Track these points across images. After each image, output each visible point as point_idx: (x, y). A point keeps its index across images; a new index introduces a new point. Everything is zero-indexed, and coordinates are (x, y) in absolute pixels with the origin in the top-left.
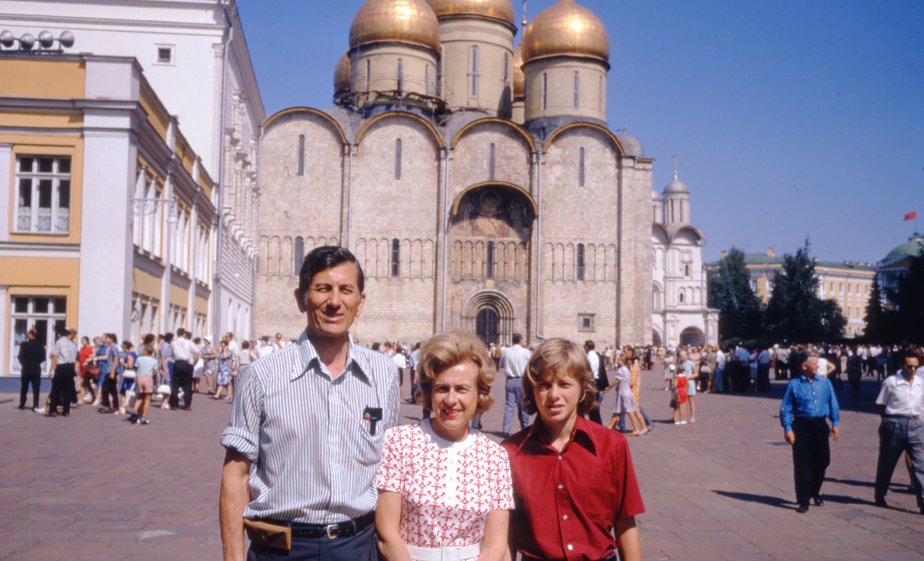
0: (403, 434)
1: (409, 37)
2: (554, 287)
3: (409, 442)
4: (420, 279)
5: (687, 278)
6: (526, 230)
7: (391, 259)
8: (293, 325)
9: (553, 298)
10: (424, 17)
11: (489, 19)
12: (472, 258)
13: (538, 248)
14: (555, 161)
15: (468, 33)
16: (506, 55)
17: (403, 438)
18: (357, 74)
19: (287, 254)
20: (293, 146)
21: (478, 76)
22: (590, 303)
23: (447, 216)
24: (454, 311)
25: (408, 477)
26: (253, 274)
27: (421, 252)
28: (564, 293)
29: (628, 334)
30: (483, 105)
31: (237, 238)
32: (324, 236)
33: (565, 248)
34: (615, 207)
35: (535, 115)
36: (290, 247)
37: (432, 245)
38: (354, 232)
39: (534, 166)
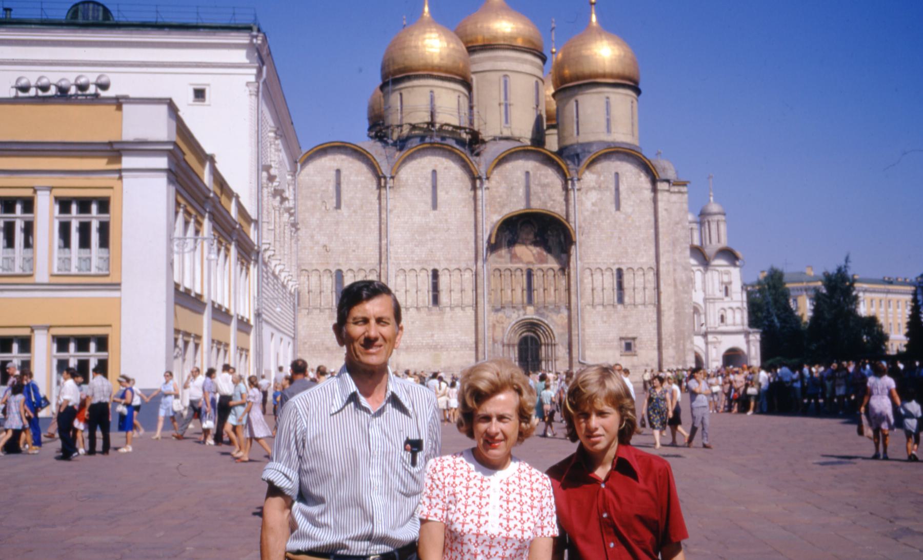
0: (445, 464)
1: (439, 68)
2: (594, 312)
3: (452, 472)
5: (727, 299)
6: (564, 256)
7: (431, 289)
10: (454, 49)
12: (512, 286)
15: (499, 63)
17: (446, 468)
18: (390, 107)
19: (327, 287)
21: (510, 105)
23: (485, 245)
25: (451, 506)
26: (294, 307)
30: (517, 134)
31: (277, 273)
32: (363, 268)
33: (604, 272)
34: (652, 231)
35: (568, 142)
36: (330, 280)
37: (471, 274)
38: (393, 264)
39: (570, 192)
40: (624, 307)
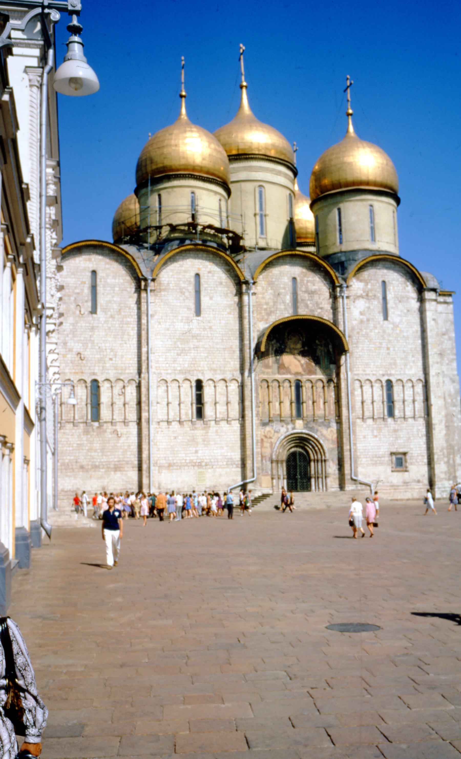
1: (201, 169)
2: (365, 426)
4: (226, 421)
7: (194, 401)
8: (91, 477)
9: (364, 437)
11: (273, 159)
12: (280, 398)
13: (347, 385)
14: (358, 295)
16: (290, 194)
18: (149, 207)
21: (265, 216)
22: (402, 441)
24: (264, 455)
27: (226, 393)
28: (375, 431)
29: (442, 472)
32: (122, 378)
33: (374, 384)
34: (420, 342)
36: (85, 391)
37: (237, 385)
38: (155, 373)
39: (338, 299)
40: (395, 421)
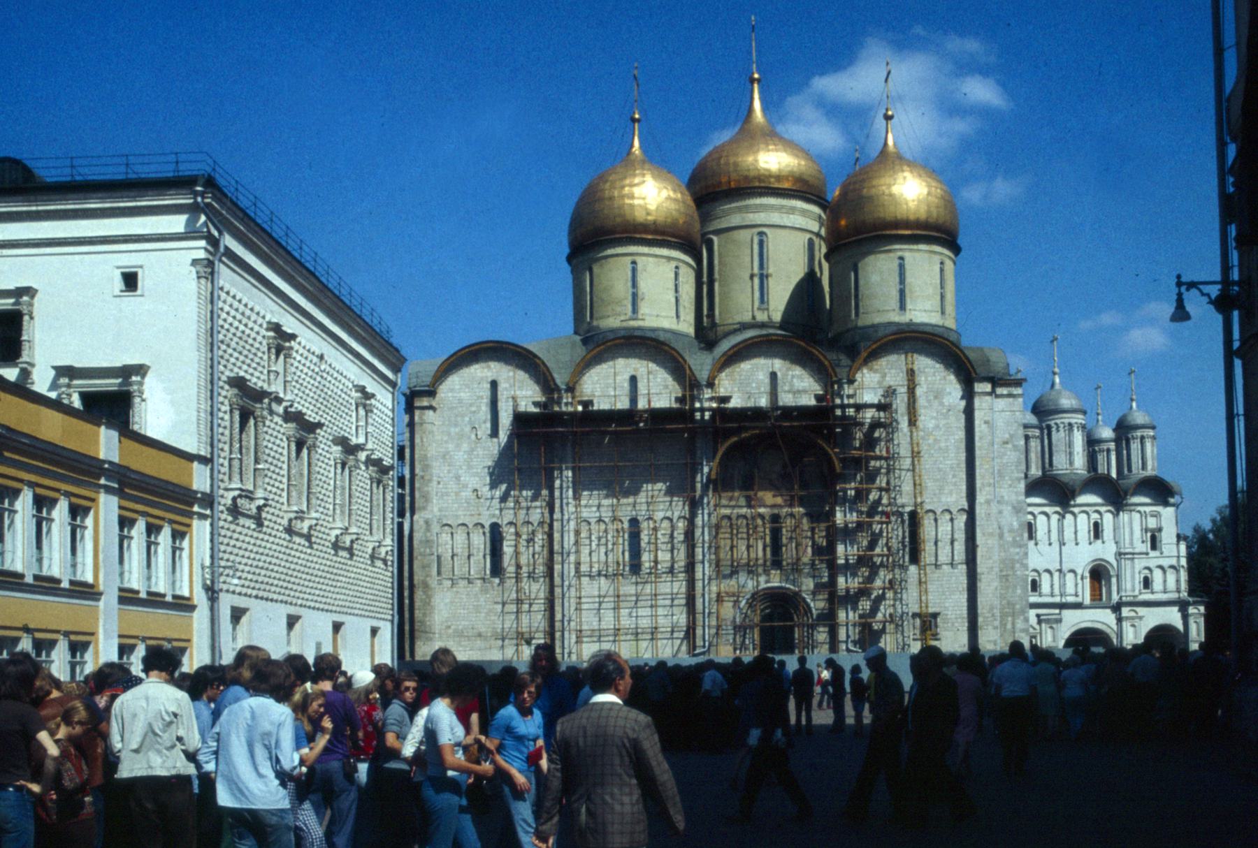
5: (1152, 554)
10: (669, 198)
15: (762, 215)
19: (479, 549)
20: (482, 397)
